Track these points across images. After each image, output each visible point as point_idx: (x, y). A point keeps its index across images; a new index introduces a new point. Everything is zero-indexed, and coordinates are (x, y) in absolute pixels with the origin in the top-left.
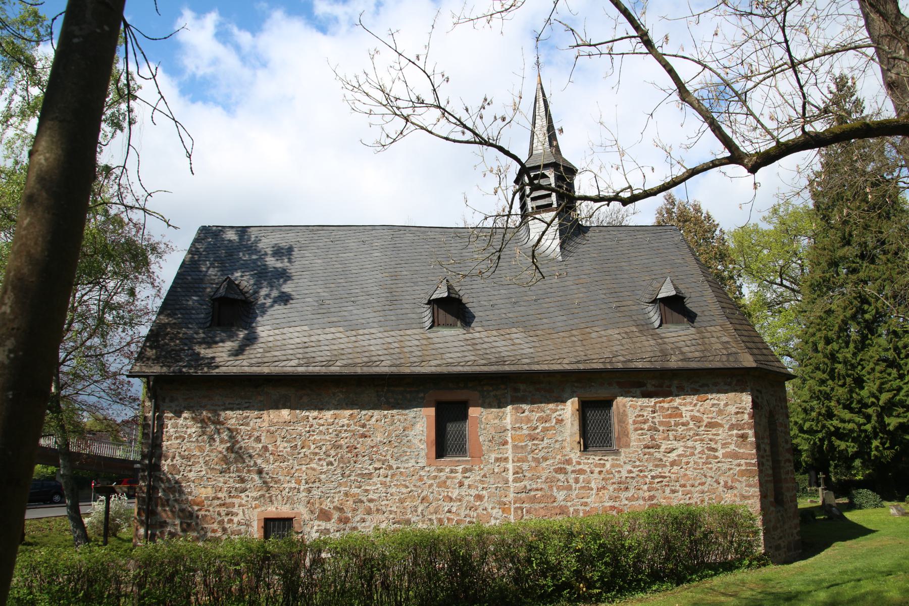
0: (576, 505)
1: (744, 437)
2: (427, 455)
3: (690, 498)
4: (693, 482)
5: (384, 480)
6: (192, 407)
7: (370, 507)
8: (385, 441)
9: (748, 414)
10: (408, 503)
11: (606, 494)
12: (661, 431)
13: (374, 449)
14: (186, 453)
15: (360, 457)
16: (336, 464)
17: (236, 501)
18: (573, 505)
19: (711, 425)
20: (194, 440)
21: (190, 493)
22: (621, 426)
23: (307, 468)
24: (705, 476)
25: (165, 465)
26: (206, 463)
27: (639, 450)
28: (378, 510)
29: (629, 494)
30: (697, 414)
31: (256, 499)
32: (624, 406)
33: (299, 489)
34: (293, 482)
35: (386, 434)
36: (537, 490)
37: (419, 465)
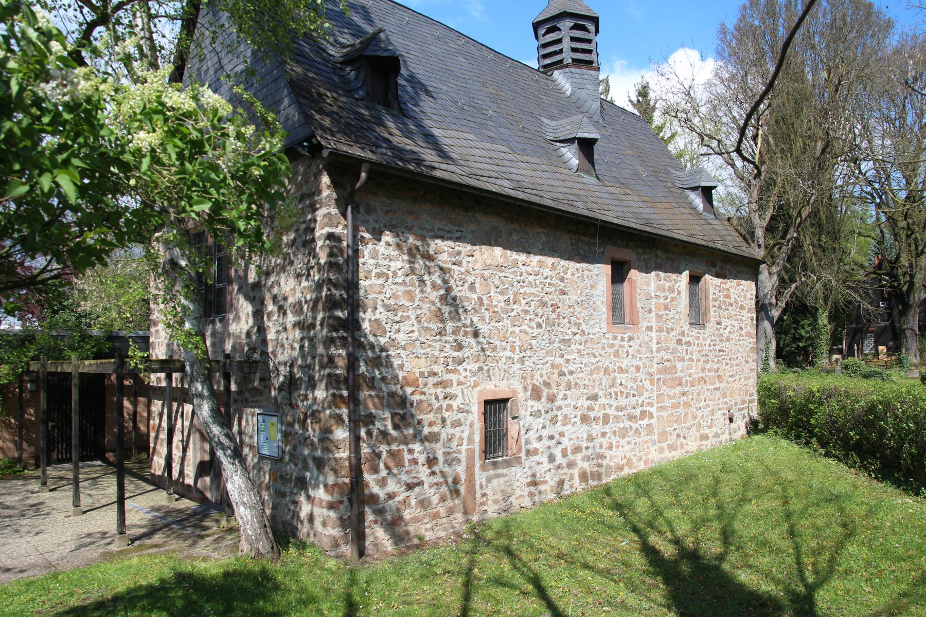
17: (453, 377)
20: (400, 280)
21: (401, 367)
25: (367, 320)
31: (474, 374)
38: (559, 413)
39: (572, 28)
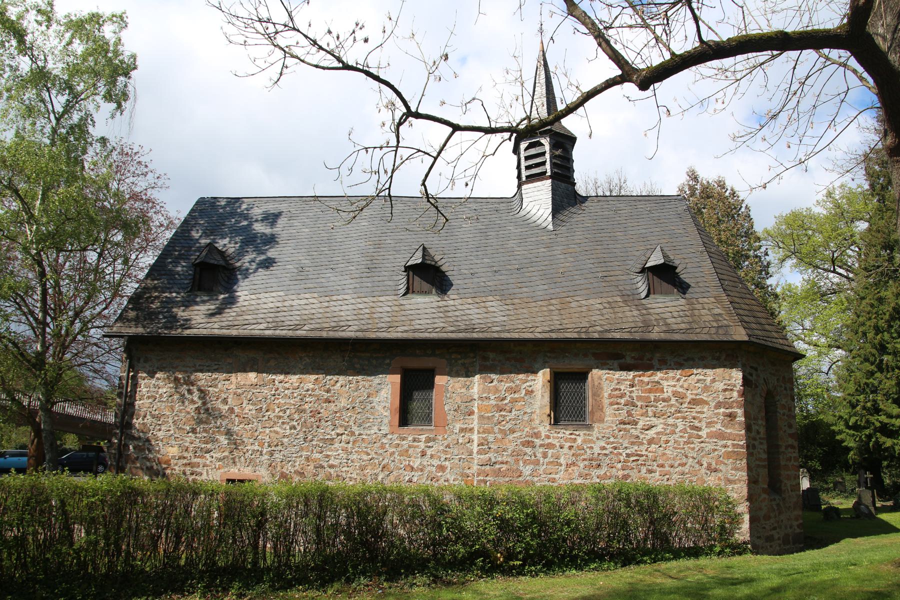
0: (543, 481)
1: (732, 416)
3: (668, 480)
4: (673, 462)
5: (346, 446)
6: (164, 368)
7: (330, 473)
8: (348, 406)
9: (738, 391)
12: (639, 406)
14: (157, 412)
15: (323, 422)
16: (299, 428)
19: (694, 402)
21: (159, 451)
22: (596, 400)
23: (271, 431)
24: (686, 457)
25: (137, 422)
27: (614, 425)
28: (338, 476)
29: (601, 472)
30: (681, 390)
31: (220, 460)
32: (600, 378)
33: (261, 452)
34: (256, 444)
35: (350, 400)
36: (502, 463)
37: (382, 432)
39: (526, 150)
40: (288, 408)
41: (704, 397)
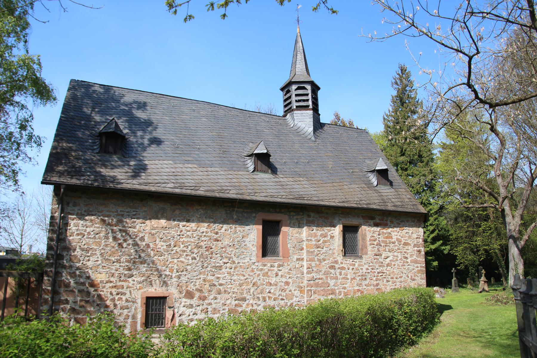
0: (340, 289)
1: (419, 251)
2: (257, 254)
5: (230, 270)
8: (230, 244)
9: (422, 239)
10: (244, 287)
11: (355, 282)
13: (224, 249)
14: (86, 247)
15: (214, 255)
16: (198, 259)
18: (338, 289)
19: (406, 244)
23: (178, 261)
26: (102, 254)
27: (372, 256)
28: (225, 291)
29: (366, 282)
30: (399, 237)
31: (140, 283)
32: (365, 230)
33: (171, 276)
35: (231, 240)
37: (252, 261)
38: (209, 307)
39: (296, 90)
40: (190, 245)
41: (409, 241)
